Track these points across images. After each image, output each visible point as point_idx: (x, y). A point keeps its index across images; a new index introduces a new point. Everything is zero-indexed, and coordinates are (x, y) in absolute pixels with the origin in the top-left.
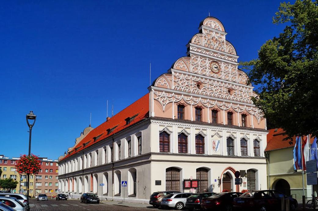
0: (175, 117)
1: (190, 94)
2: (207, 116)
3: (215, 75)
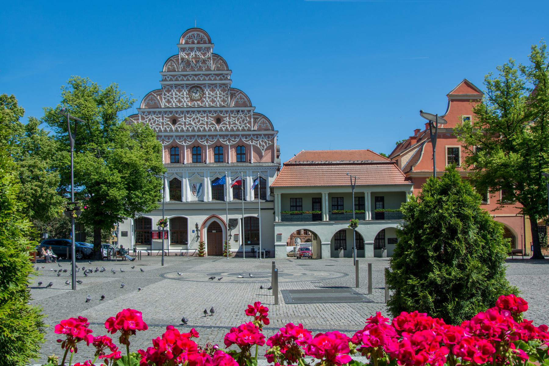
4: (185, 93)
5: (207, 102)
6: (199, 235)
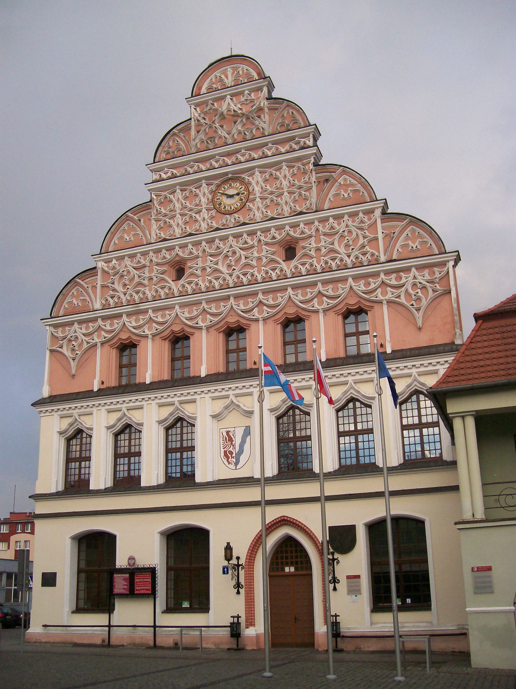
0: (103, 383)
1: (143, 306)
3: (231, 220)
4: (204, 200)
5: (257, 209)
6: (242, 581)
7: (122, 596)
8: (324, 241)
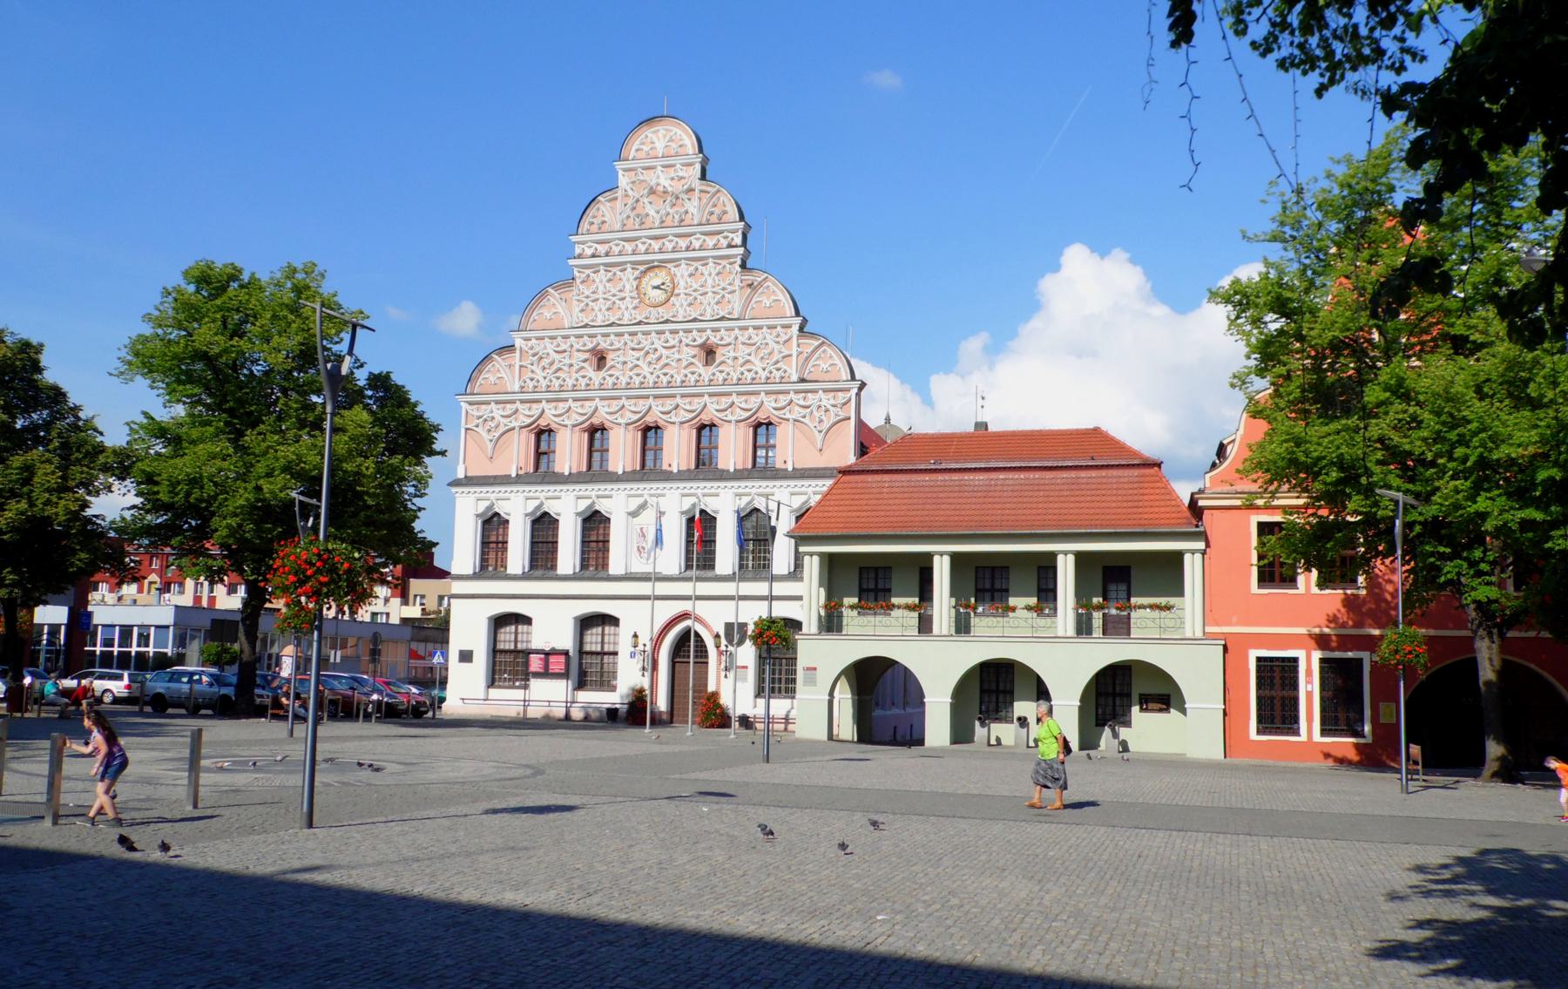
1: (563, 395)
2: (622, 451)
3: (654, 314)
7: (537, 675)
8: (743, 351)
